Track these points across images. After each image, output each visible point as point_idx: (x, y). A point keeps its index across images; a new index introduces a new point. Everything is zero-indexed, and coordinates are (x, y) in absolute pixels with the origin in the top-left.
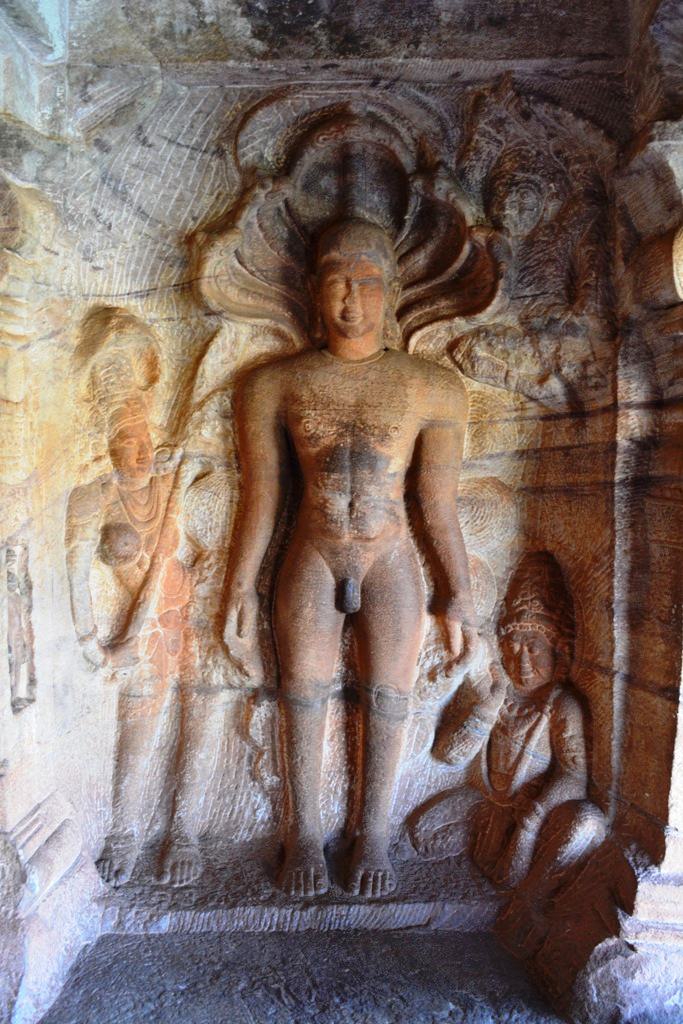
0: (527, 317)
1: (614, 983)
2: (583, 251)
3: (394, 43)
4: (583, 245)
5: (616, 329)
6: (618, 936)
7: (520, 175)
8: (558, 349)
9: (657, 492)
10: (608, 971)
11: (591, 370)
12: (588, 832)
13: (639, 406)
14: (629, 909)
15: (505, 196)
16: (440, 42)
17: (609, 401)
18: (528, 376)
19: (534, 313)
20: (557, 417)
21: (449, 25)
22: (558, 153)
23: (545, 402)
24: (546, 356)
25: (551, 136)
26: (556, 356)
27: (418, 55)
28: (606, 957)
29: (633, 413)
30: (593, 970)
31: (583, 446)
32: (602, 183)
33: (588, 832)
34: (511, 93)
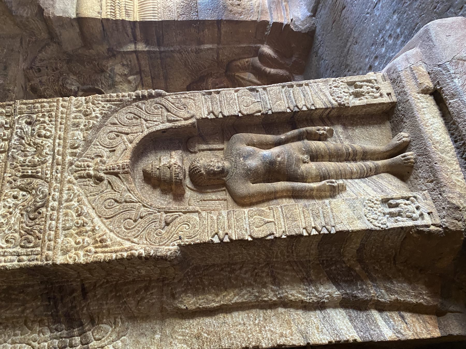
0: (109, 86)
1: (303, 22)
2: (87, 67)
3: (8, 97)
4: (85, 66)
5: (113, 54)
6: (289, 25)
7: (60, 83)
8: (119, 75)
9: (161, 38)
10: (300, 25)
11: (125, 63)
12: (266, 49)
13: (135, 44)
14: (282, 24)
15: (67, 89)
16: (10, 83)
17: (134, 55)
18: (128, 88)
19: (107, 83)
20: (141, 79)
21: (4, 81)
22: (54, 71)
23: (137, 83)
24: (121, 80)
25: (47, 67)
26: (121, 75)
27: (14, 90)
28: (296, 26)
29: (137, 47)
30: (301, 29)
31: (151, 71)
32: (64, 60)
33: (266, 49)
34: (31, 71)
